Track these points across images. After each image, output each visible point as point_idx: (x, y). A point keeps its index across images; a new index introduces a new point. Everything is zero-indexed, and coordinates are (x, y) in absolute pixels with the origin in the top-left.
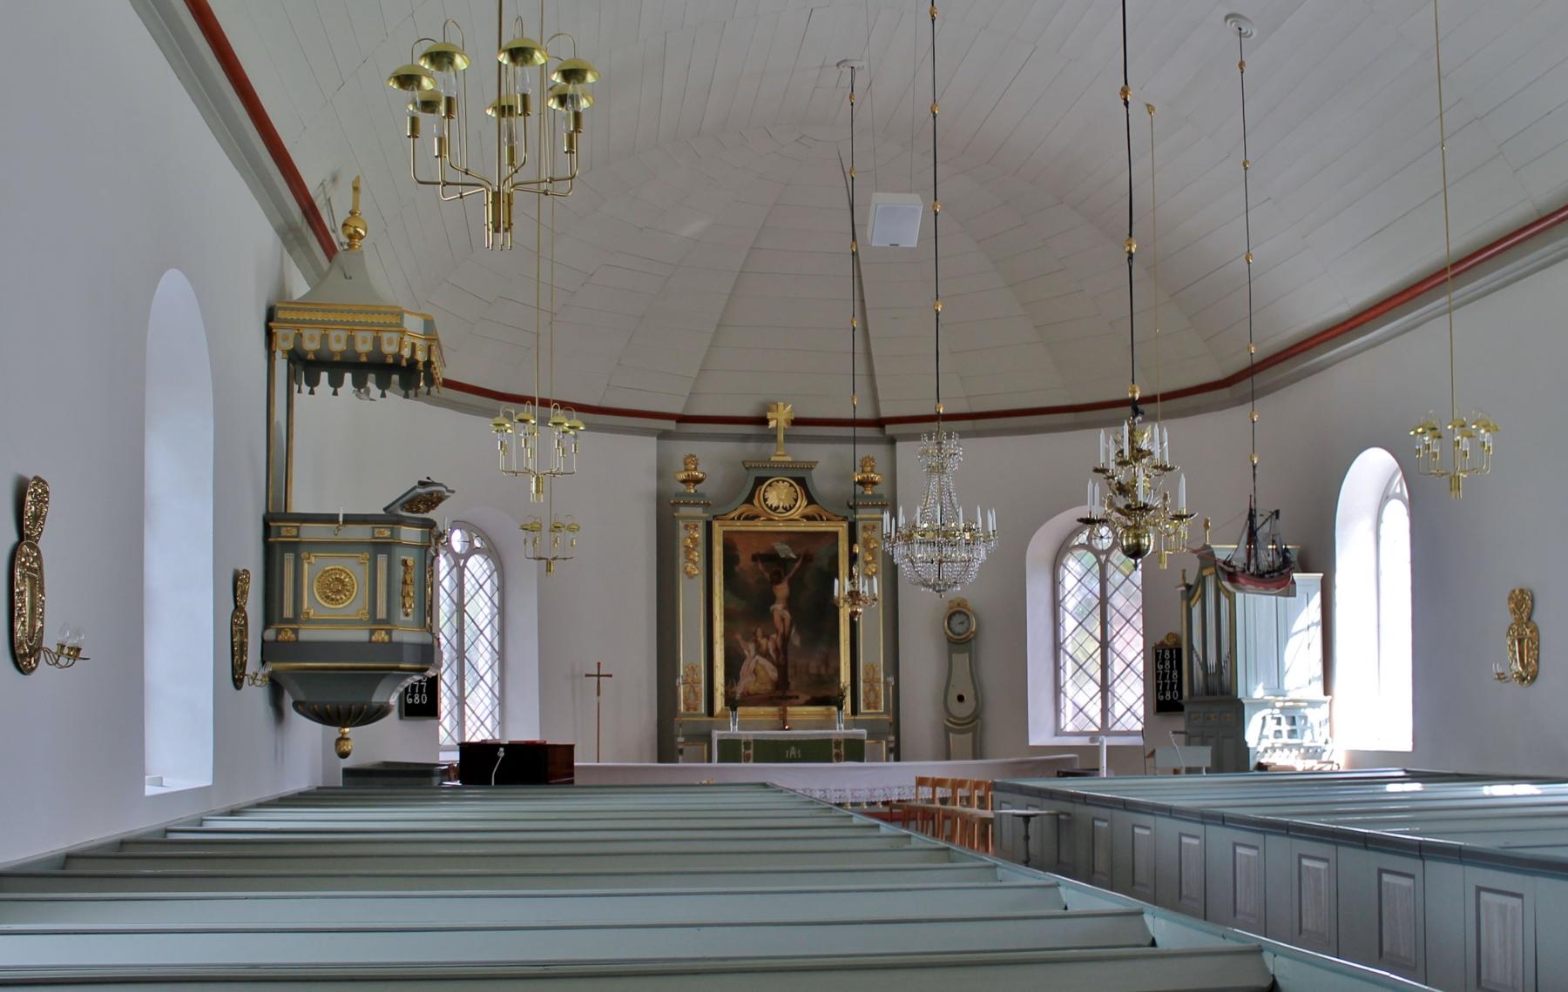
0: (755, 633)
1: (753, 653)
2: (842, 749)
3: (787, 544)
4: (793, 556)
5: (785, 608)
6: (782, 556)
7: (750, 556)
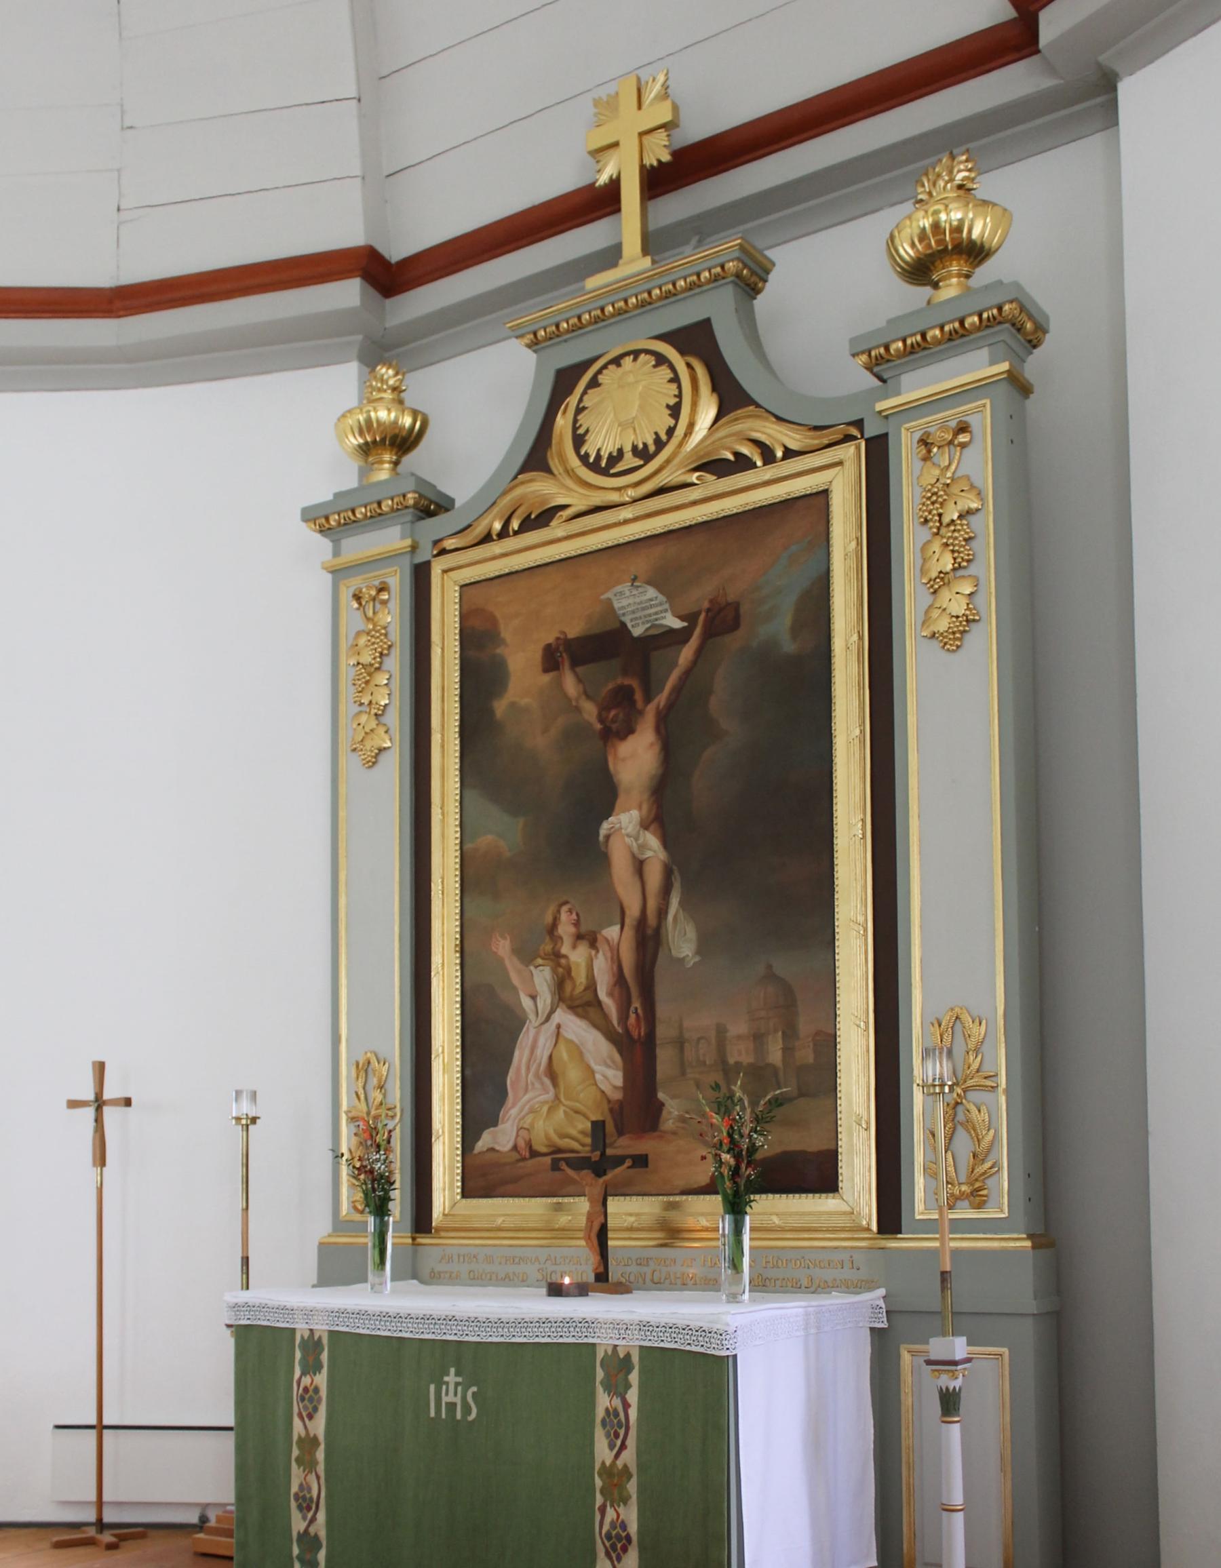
0: (552, 929)
1: (545, 998)
2: (633, 1396)
3: (649, 583)
5: (645, 826)
6: (637, 632)
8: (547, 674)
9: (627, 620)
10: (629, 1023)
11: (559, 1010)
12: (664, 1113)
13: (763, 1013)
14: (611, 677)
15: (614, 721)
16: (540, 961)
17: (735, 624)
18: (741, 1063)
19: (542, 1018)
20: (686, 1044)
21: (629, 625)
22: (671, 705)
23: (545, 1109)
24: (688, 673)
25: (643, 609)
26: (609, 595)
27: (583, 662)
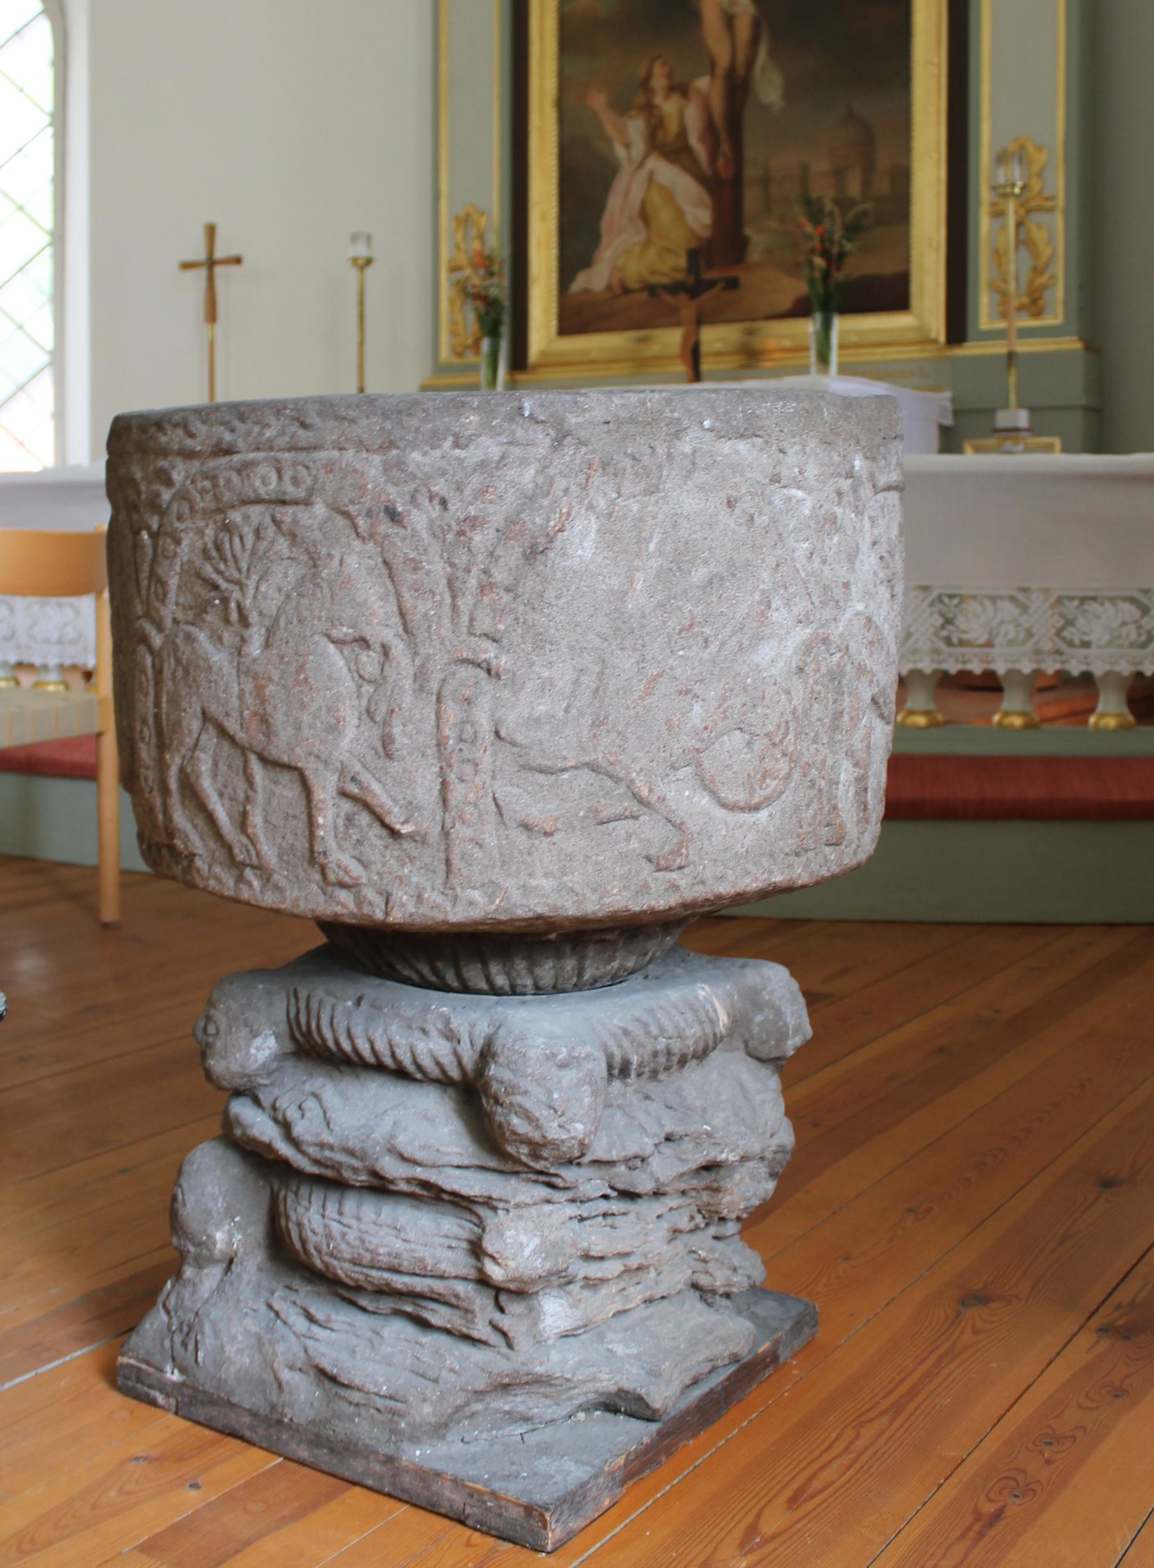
0: (645, 85)
1: (639, 146)
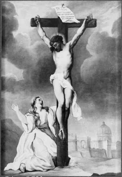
0: (33, 105)
1: (31, 125)
3: (68, 7)
4: (78, 22)
7: (30, 21)
8: (32, 27)
9: (60, 16)
10: (59, 135)
11: (35, 129)
12: (71, 161)
13: (102, 135)
14: (54, 32)
15: (55, 46)
16: (28, 114)
17: (95, 25)
18: (95, 148)
19: (30, 130)
20: (78, 142)
21: (61, 19)
22: (74, 45)
23: (31, 157)
24: (80, 36)
25: (66, 14)
26: (54, 7)
27: (46, 26)
